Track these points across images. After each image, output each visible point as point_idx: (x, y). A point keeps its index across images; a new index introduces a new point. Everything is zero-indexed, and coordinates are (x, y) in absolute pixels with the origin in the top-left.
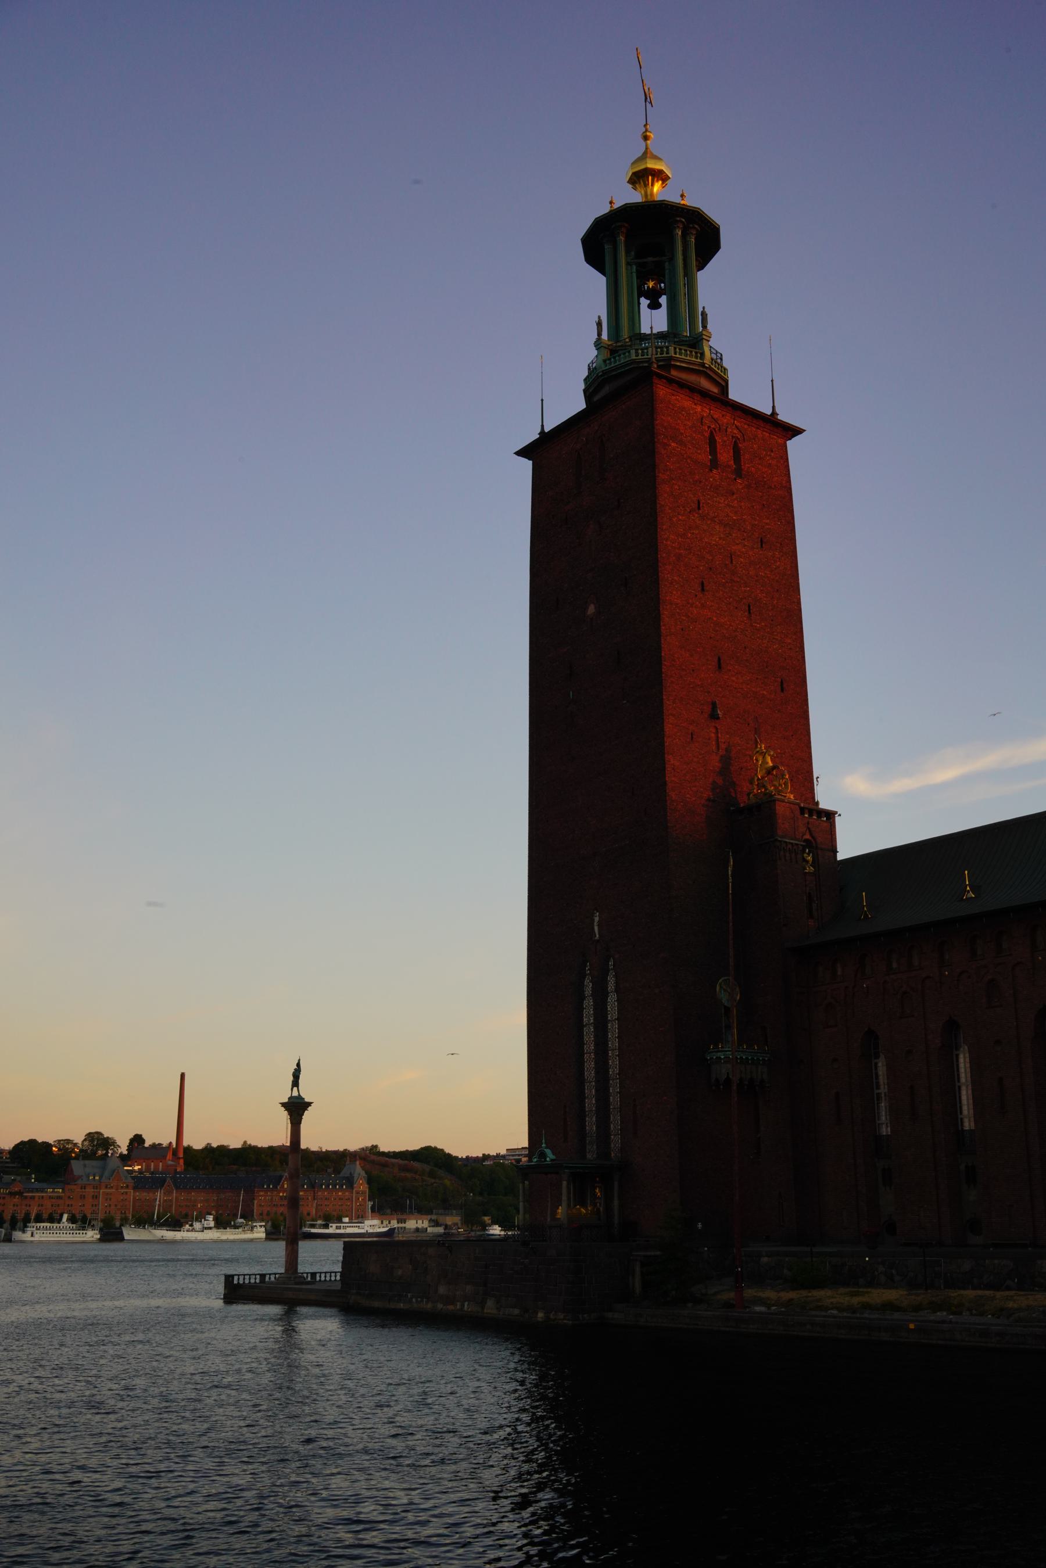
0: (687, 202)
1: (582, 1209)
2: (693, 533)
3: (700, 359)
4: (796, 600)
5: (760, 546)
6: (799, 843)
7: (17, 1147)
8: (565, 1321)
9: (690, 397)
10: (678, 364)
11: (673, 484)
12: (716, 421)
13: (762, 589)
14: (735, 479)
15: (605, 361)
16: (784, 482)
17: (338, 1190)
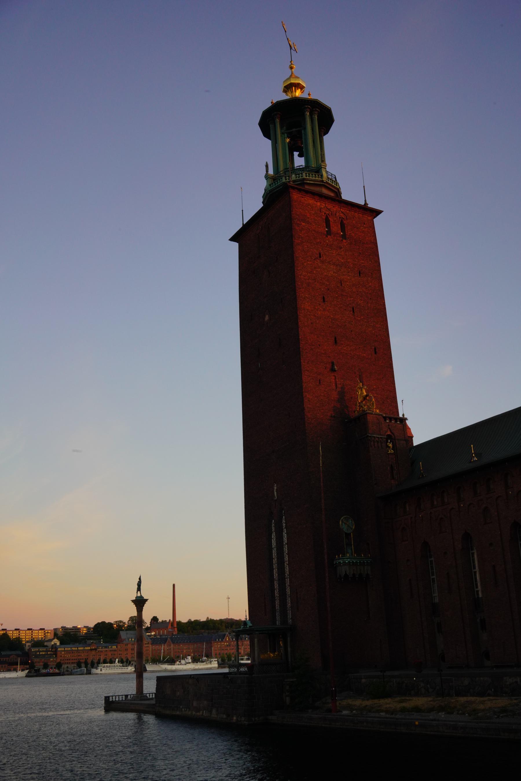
0: (312, 97)
1: (271, 654)
2: (317, 271)
3: (321, 178)
4: (382, 303)
5: (359, 275)
6: (382, 437)
7: (96, 625)
8: (245, 722)
9: (312, 198)
10: (308, 182)
11: (304, 245)
12: (329, 210)
13: (361, 298)
14: (342, 240)
15: (270, 185)
16: (372, 240)
17: (221, 642)
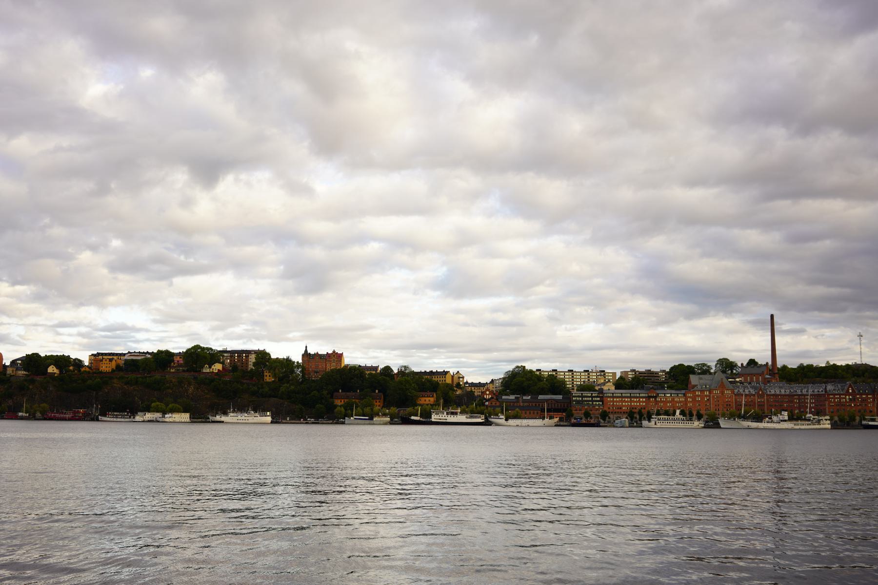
7: (672, 369)
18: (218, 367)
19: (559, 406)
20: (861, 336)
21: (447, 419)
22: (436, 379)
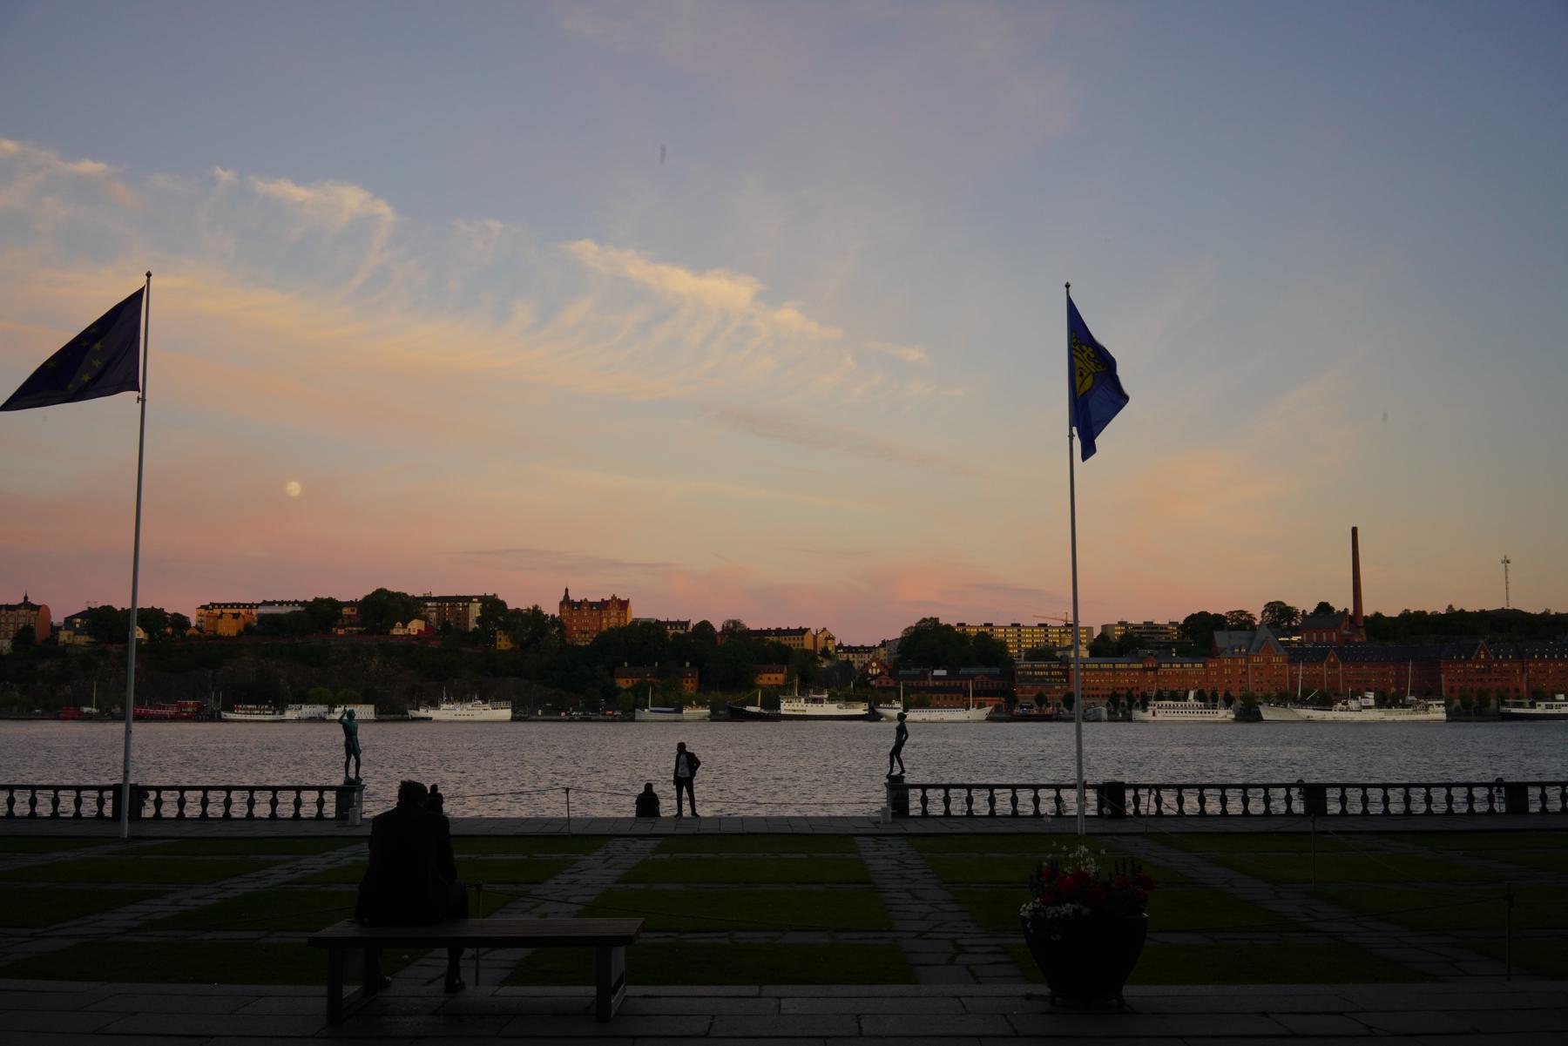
7: (1188, 620)
18: (416, 626)
19: (995, 686)
20: (1508, 562)
21: (805, 711)
22: (787, 643)
